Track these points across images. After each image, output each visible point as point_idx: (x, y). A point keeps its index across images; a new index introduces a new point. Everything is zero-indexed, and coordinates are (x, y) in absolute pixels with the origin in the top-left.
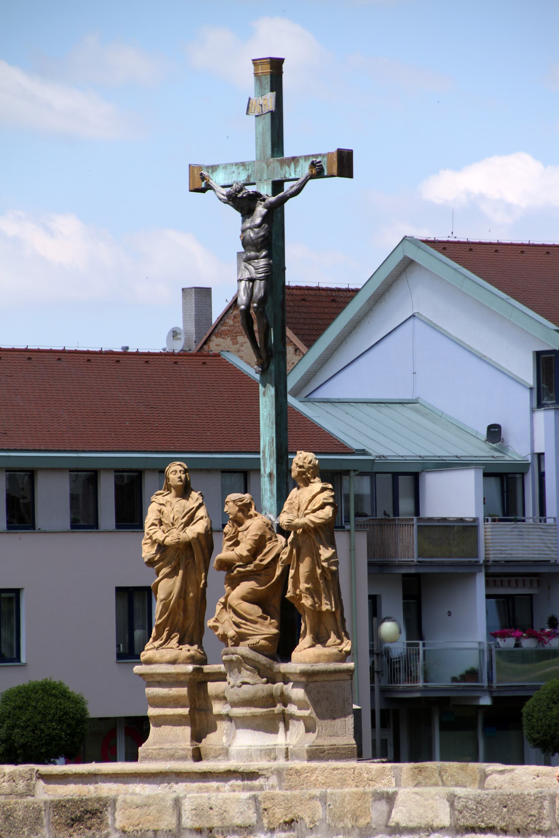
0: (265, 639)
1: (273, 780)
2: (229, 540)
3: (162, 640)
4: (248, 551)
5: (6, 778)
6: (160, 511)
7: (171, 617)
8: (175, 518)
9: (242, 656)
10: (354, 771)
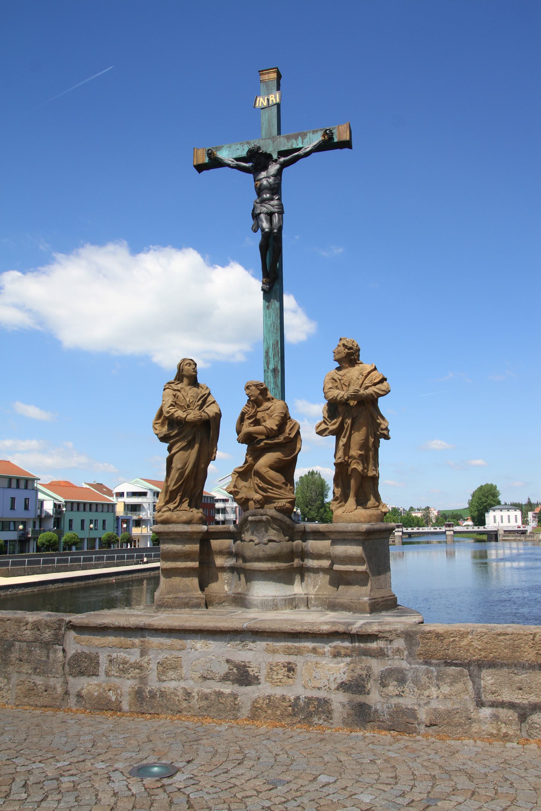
0: (289, 502)
1: (400, 643)
2: (249, 418)
3: (175, 503)
4: (277, 425)
5: (29, 626)
6: (175, 396)
7: (184, 484)
8: (191, 401)
9: (272, 517)
10: (534, 637)
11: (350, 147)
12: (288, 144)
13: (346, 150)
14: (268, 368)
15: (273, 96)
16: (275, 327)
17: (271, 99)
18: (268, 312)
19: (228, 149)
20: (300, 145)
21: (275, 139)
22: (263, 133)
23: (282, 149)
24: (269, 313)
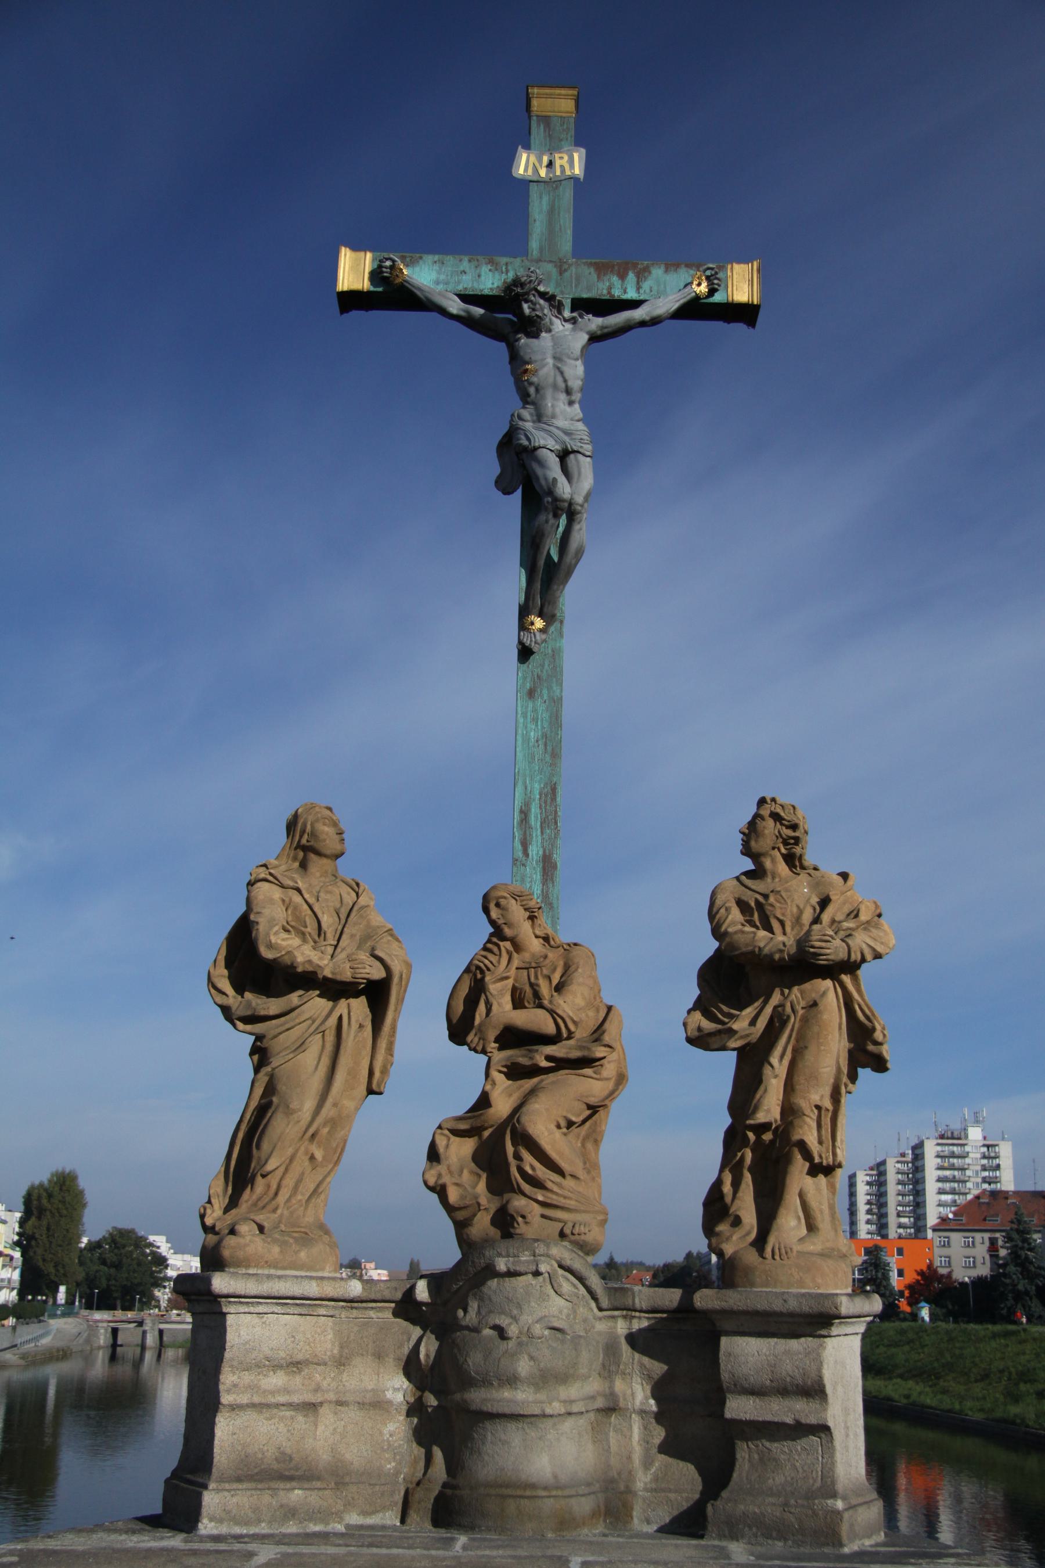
11: (751, 322)
12: (600, 285)
13: (740, 328)
14: (526, 854)
15: (566, 158)
16: (549, 749)
17: (558, 163)
18: (531, 705)
19: (436, 267)
20: (631, 294)
21: (566, 266)
22: (534, 245)
23: (585, 296)
24: (535, 710)
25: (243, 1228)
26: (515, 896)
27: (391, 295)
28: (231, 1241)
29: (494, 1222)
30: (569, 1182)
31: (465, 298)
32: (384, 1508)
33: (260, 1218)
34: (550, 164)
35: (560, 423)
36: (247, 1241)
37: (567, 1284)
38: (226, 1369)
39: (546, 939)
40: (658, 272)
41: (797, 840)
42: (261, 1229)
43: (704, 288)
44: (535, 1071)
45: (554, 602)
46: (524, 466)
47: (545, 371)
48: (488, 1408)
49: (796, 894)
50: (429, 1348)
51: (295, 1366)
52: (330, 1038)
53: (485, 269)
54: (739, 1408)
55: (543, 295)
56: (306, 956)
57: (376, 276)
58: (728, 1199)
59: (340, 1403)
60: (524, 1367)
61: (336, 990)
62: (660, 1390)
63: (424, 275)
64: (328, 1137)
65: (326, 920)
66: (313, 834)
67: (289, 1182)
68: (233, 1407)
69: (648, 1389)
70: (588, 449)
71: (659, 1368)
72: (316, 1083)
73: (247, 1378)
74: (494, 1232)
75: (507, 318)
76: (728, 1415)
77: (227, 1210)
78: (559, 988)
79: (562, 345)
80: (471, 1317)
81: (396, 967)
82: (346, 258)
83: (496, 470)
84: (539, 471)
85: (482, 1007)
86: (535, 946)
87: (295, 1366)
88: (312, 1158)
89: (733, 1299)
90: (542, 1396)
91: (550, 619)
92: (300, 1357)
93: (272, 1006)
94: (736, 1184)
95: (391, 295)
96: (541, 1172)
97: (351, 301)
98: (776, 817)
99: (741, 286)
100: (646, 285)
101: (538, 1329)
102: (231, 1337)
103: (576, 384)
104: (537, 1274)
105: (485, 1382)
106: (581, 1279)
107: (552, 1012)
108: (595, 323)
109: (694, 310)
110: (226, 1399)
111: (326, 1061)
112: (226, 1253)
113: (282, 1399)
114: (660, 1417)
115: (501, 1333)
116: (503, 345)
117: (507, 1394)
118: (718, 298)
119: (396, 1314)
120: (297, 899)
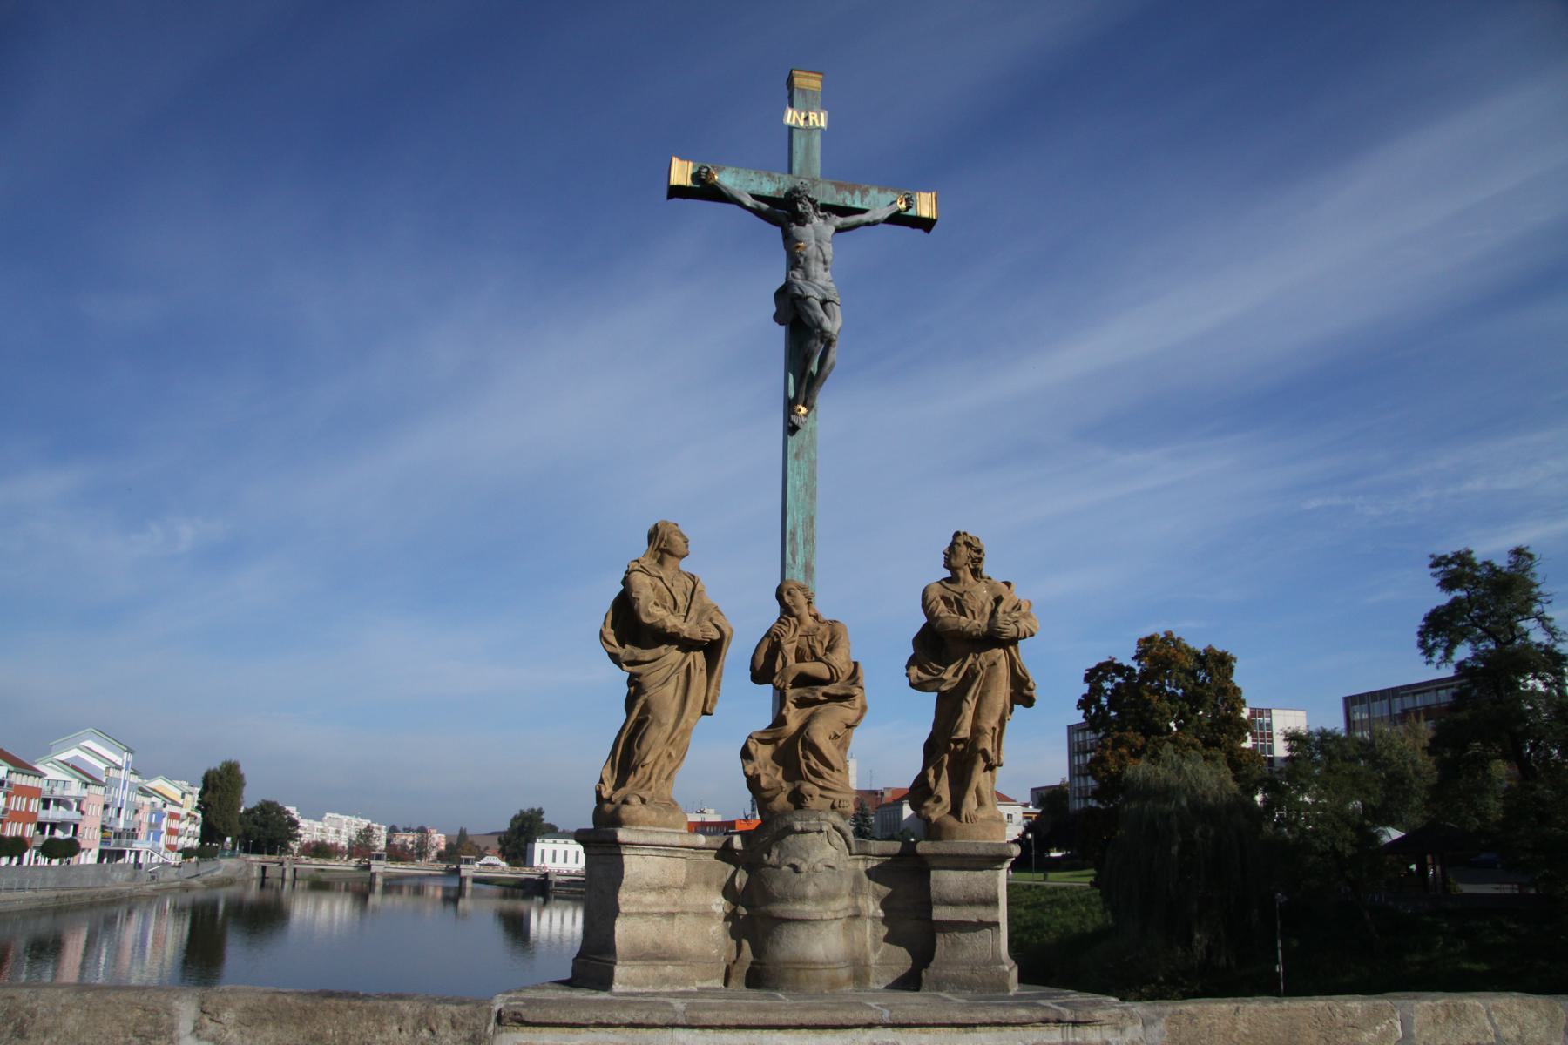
13: (919, 232)
20: (858, 205)
25: (635, 800)
26: (801, 588)
27: (705, 190)
28: (625, 808)
29: (789, 799)
30: (836, 774)
31: (755, 197)
32: (713, 977)
33: (642, 794)
34: (806, 118)
35: (820, 282)
36: (634, 809)
37: (837, 839)
38: (622, 890)
39: (816, 617)
40: (874, 192)
41: (980, 560)
42: (643, 801)
43: (904, 206)
44: (817, 702)
45: (813, 398)
46: (795, 307)
47: (811, 249)
48: (787, 915)
49: (980, 595)
50: (741, 879)
51: (663, 889)
52: (682, 677)
53: (765, 179)
54: (940, 913)
55: (810, 200)
56: (673, 622)
57: (696, 177)
58: (932, 785)
59: (683, 913)
60: (811, 890)
61: (687, 645)
62: (885, 904)
63: (726, 179)
64: (678, 743)
65: (680, 599)
66: (669, 541)
67: (656, 771)
68: (627, 914)
69: (878, 904)
70: (838, 300)
71: (885, 890)
72: (674, 706)
73: (634, 896)
74: (790, 806)
75: (784, 212)
76: (934, 918)
77: (616, 788)
78: (829, 649)
79: (817, 232)
80: (774, 859)
81: (727, 632)
82: (676, 164)
83: (774, 309)
84: (810, 312)
85: (779, 661)
86: (809, 621)
87: (663, 889)
88: (670, 755)
89: (942, 847)
90: (820, 908)
91: (810, 407)
92: (667, 883)
93: (647, 654)
94: (937, 777)
95: (705, 190)
96: (821, 768)
97: (677, 192)
98: (968, 544)
99: (925, 206)
100: (867, 200)
101: (820, 866)
102: (626, 869)
103: (829, 258)
104: (820, 831)
105: (784, 900)
106: (844, 835)
107: (828, 665)
108: (839, 221)
109: (897, 219)
110: (623, 909)
111: (680, 692)
112: (624, 816)
113: (656, 910)
114: (885, 921)
115: (796, 869)
116: (778, 230)
117: (798, 907)
118: (911, 212)
119: (717, 857)
120: (660, 584)
